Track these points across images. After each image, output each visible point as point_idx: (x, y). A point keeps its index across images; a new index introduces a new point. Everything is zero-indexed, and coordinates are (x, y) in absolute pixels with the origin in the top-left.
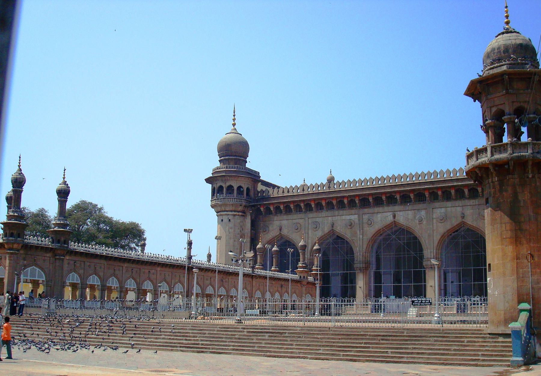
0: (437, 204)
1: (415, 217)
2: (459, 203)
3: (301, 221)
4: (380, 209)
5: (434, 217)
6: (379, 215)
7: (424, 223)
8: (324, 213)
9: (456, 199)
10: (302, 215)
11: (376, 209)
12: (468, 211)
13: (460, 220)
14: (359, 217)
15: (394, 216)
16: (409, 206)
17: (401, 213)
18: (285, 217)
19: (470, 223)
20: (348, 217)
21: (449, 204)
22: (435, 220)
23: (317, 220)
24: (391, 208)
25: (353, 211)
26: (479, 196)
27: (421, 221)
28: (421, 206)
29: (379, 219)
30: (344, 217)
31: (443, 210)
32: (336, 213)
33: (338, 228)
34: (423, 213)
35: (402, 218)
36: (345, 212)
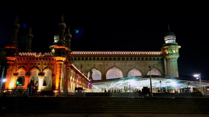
0: (128, 61)
1: (121, 64)
3: (83, 63)
4: (110, 61)
6: (110, 63)
7: (124, 66)
8: (92, 61)
10: (83, 61)
11: (109, 61)
14: (104, 64)
15: (115, 64)
16: (119, 61)
17: (117, 63)
18: (77, 61)
20: (100, 63)
21: (131, 62)
23: (89, 63)
24: (114, 61)
25: (102, 61)
27: (123, 66)
28: (122, 61)
29: (110, 65)
30: (98, 63)
31: (129, 63)
32: (96, 61)
33: (96, 66)
36: (99, 61)
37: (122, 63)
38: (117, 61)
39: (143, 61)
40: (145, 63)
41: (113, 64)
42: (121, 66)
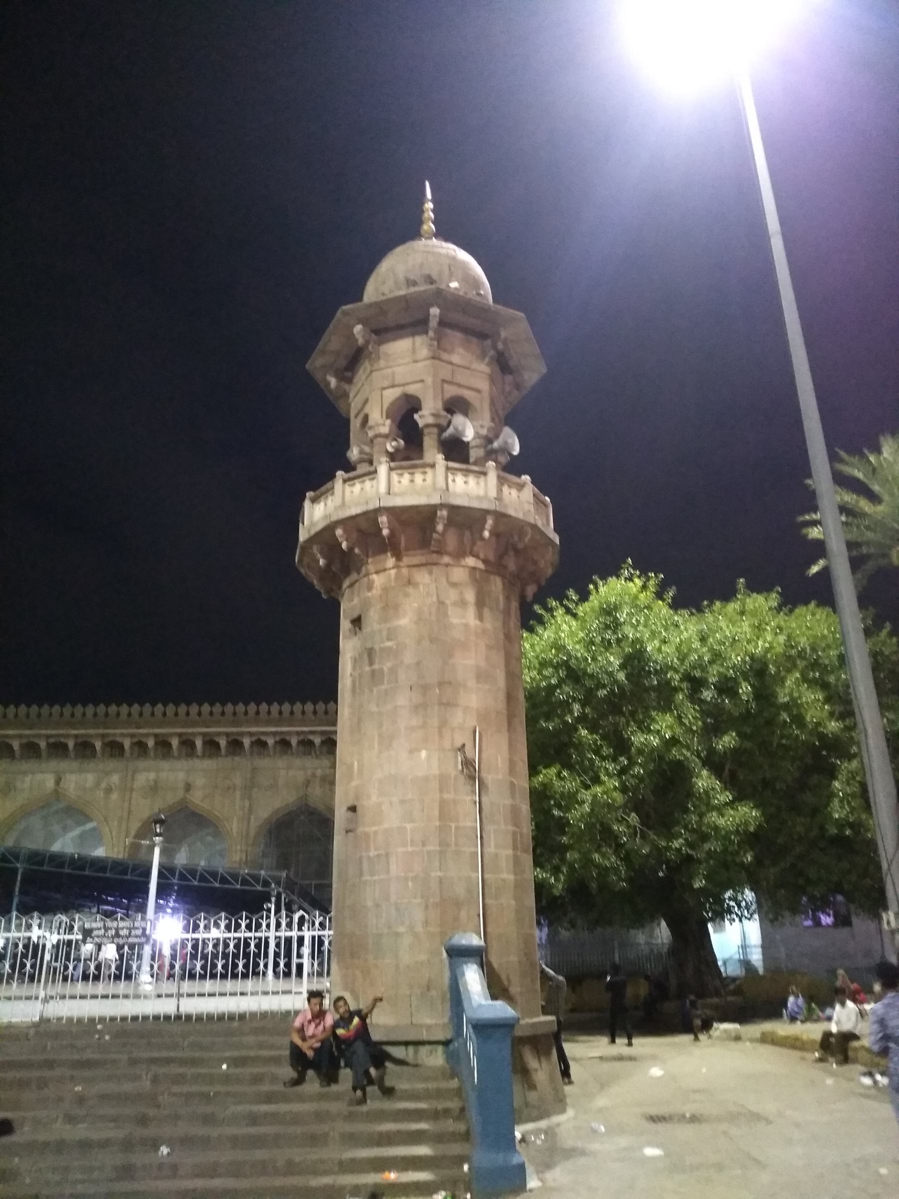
0: (142, 764)
2: (184, 764)
4: (32, 765)
5: (135, 786)
6: (28, 779)
7: (114, 796)
9: (179, 758)
11: (24, 766)
12: (199, 781)
13: (181, 794)
15: (58, 781)
19: (196, 802)
21: (165, 765)
22: (134, 794)
24: (53, 764)
26: (221, 756)
28: (111, 764)
31: (152, 776)
34: (115, 779)
35: (72, 786)
37: (108, 774)
38: (75, 765)
39: (237, 759)
40: (254, 770)
41: (50, 783)
42: (100, 794)
